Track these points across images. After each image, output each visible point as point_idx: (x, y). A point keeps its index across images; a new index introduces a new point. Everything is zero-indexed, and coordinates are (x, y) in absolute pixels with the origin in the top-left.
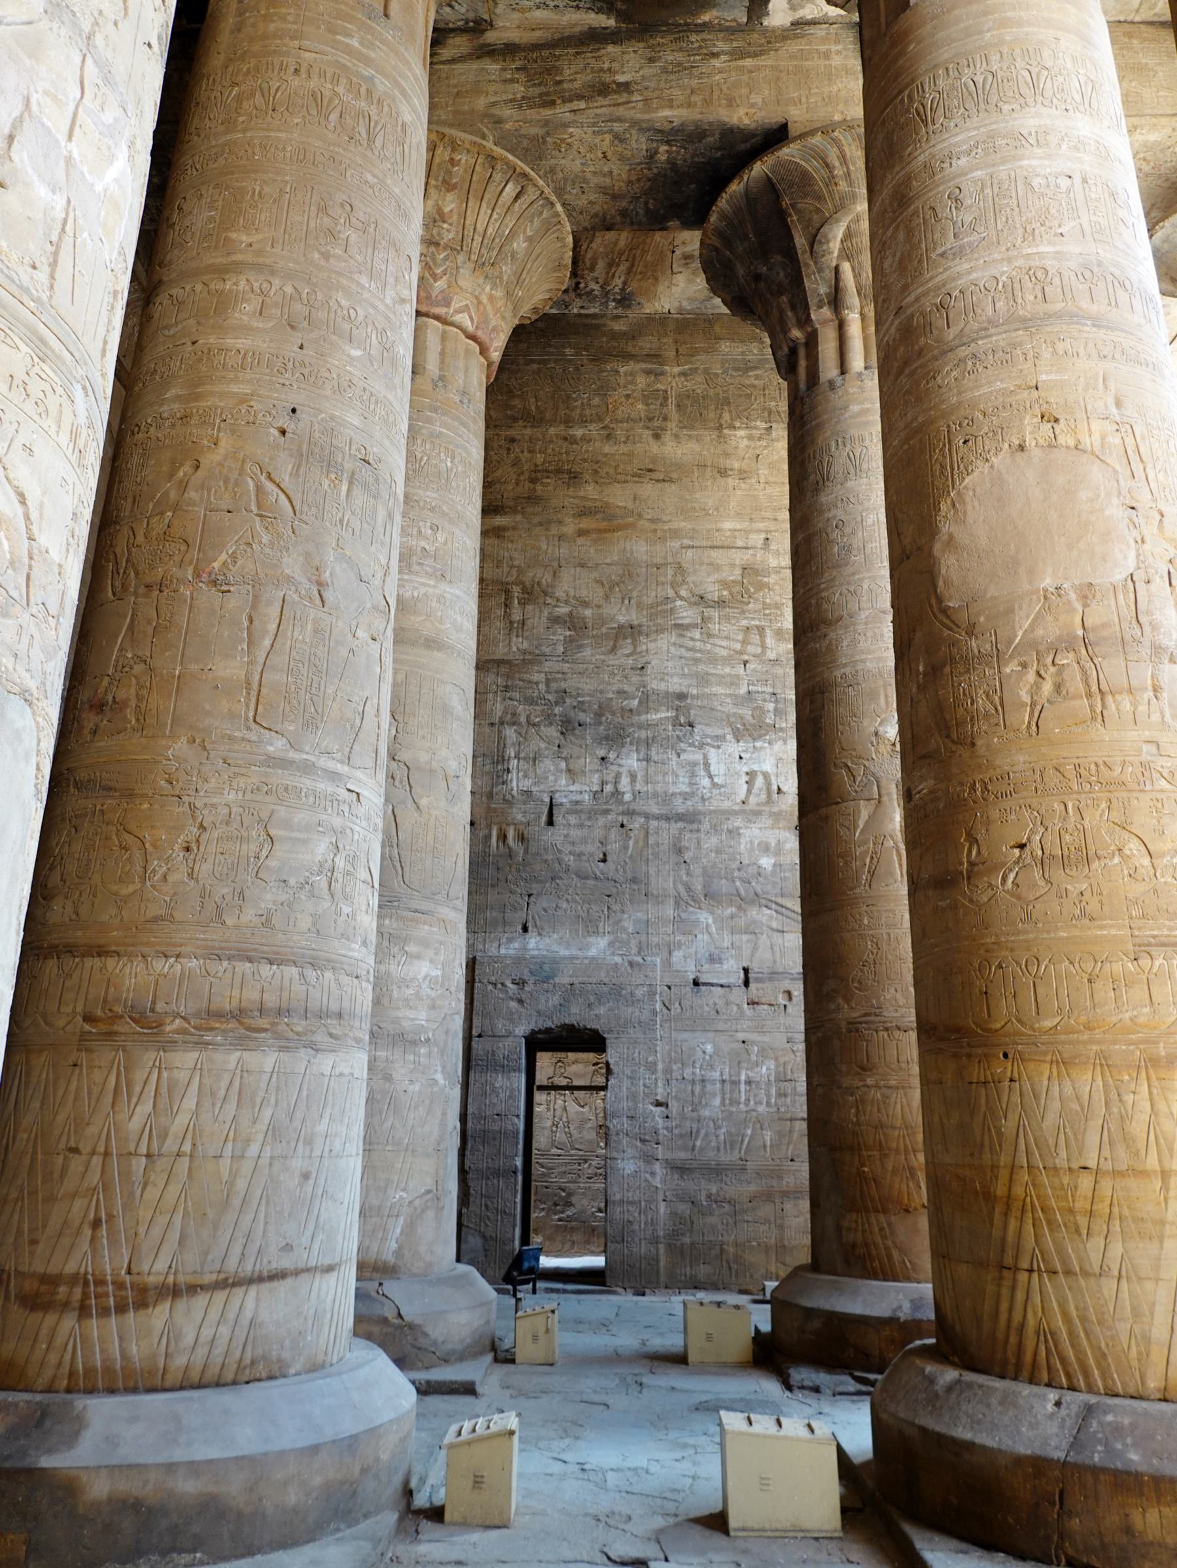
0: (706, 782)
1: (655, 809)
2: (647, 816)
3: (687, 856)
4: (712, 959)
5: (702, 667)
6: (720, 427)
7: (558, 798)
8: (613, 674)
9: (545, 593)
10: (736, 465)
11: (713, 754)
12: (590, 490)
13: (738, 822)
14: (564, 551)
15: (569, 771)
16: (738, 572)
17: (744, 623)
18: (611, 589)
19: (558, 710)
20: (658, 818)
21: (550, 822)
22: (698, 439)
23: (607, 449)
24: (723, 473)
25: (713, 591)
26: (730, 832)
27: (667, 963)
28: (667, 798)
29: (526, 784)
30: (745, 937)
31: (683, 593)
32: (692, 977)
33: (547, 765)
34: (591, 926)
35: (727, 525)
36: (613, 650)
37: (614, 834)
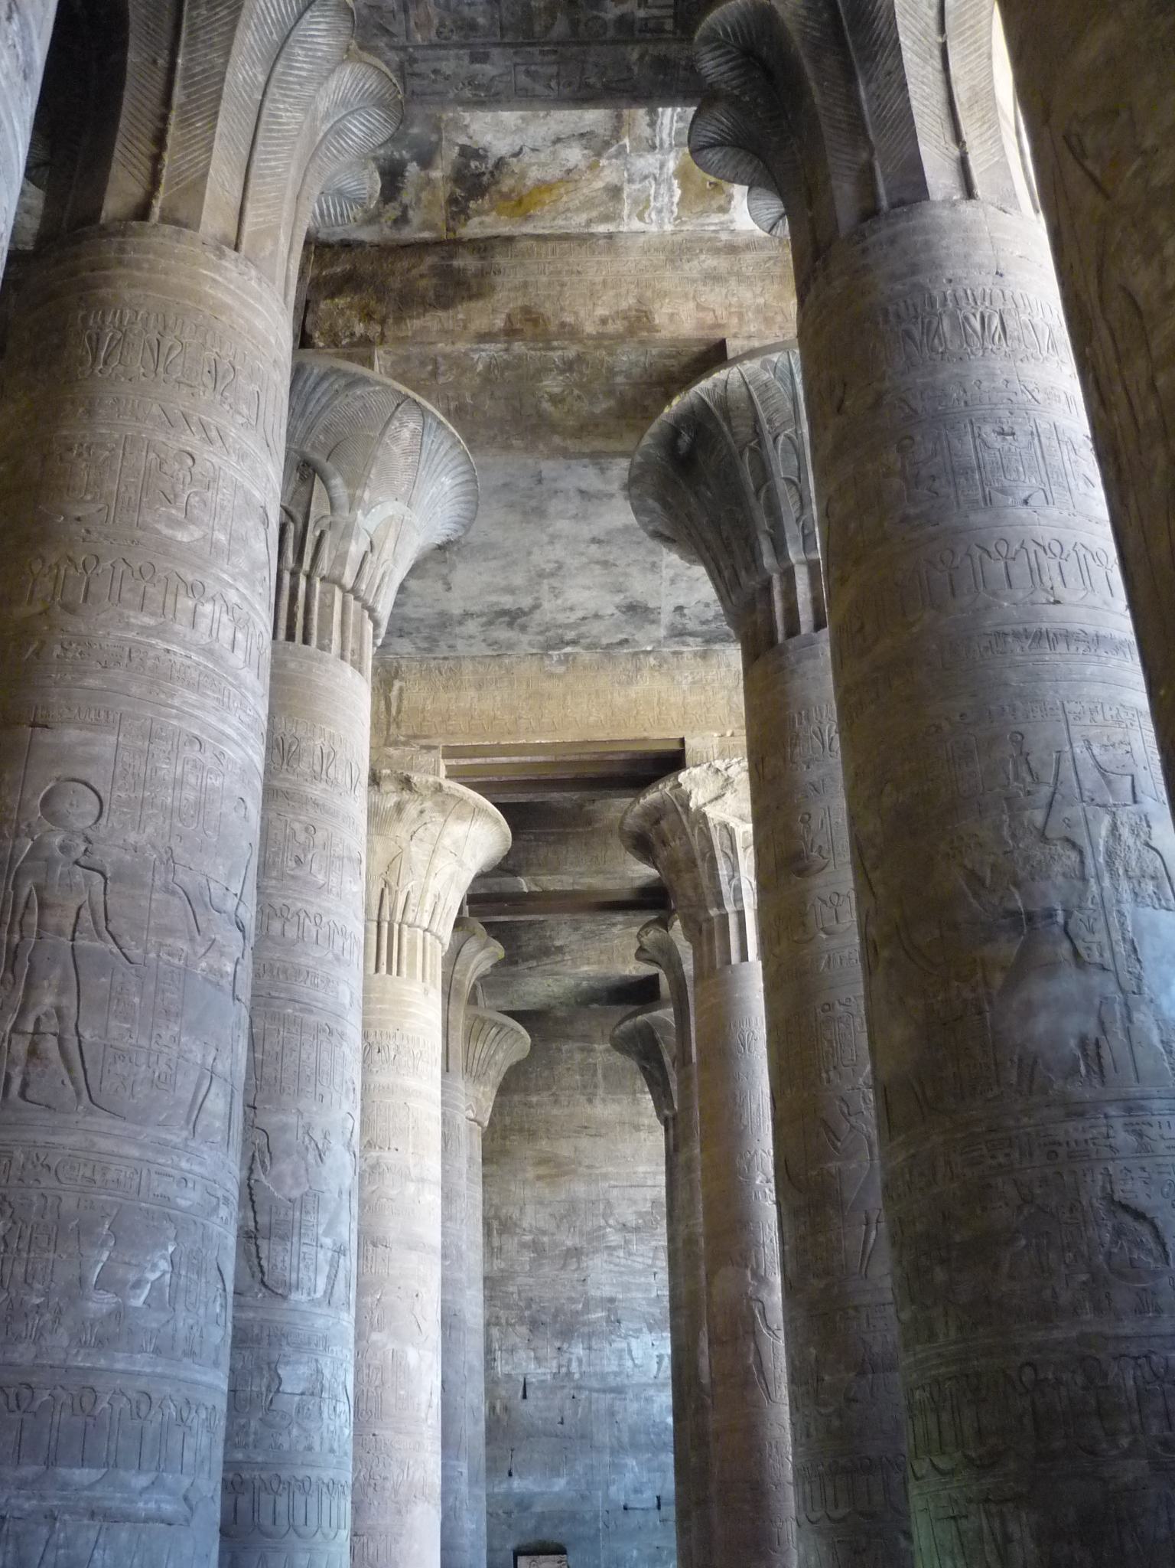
0: (629, 1363)
1: (595, 1384)
2: (591, 1390)
3: (619, 1418)
4: (636, 1491)
5: (625, 1278)
6: (634, 1093)
7: (531, 1379)
8: (564, 1285)
9: (516, 1225)
10: (646, 1122)
11: (634, 1343)
12: (544, 1144)
13: (651, 1392)
14: (528, 1192)
15: (536, 1358)
16: (649, 1205)
17: (654, 1243)
18: (561, 1219)
19: (527, 1313)
20: (598, 1391)
21: (525, 1397)
22: (619, 1101)
23: (555, 1112)
24: (637, 1128)
25: (632, 1220)
26: (646, 1399)
27: (606, 1495)
28: (603, 1376)
29: (507, 1369)
30: (658, 1474)
31: (611, 1222)
32: (622, 1504)
33: (522, 1354)
34: (555, 1472)
35: (641, 1169)
36: (564, 1267)
37: (568, 1403)
